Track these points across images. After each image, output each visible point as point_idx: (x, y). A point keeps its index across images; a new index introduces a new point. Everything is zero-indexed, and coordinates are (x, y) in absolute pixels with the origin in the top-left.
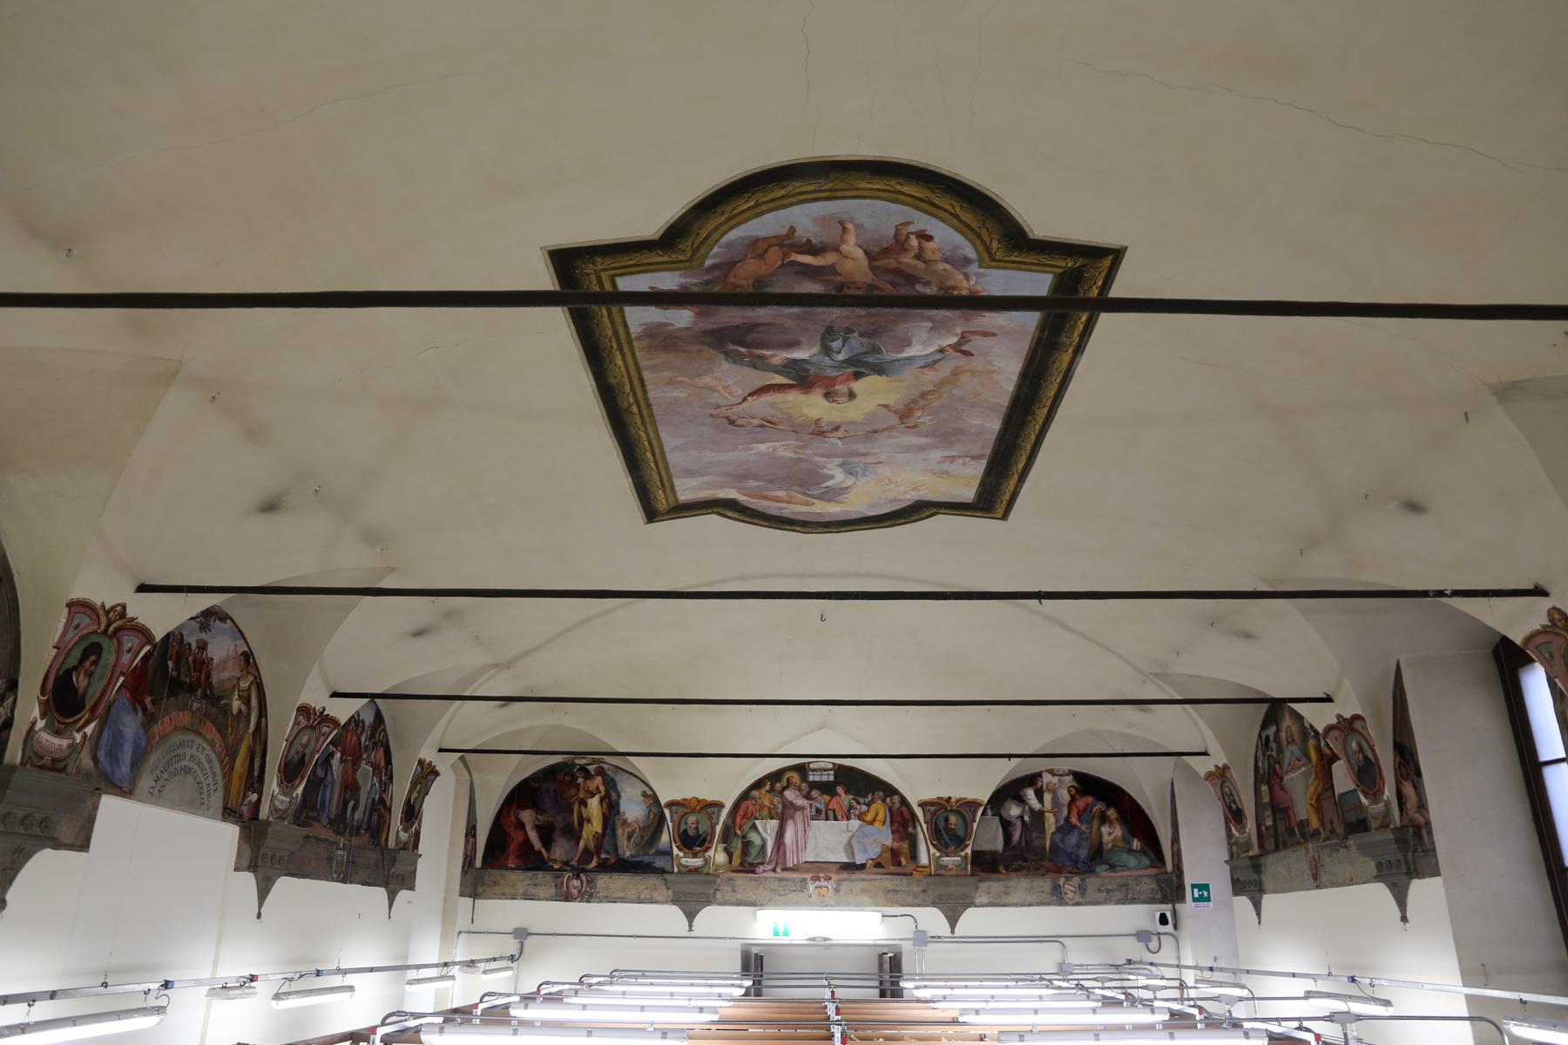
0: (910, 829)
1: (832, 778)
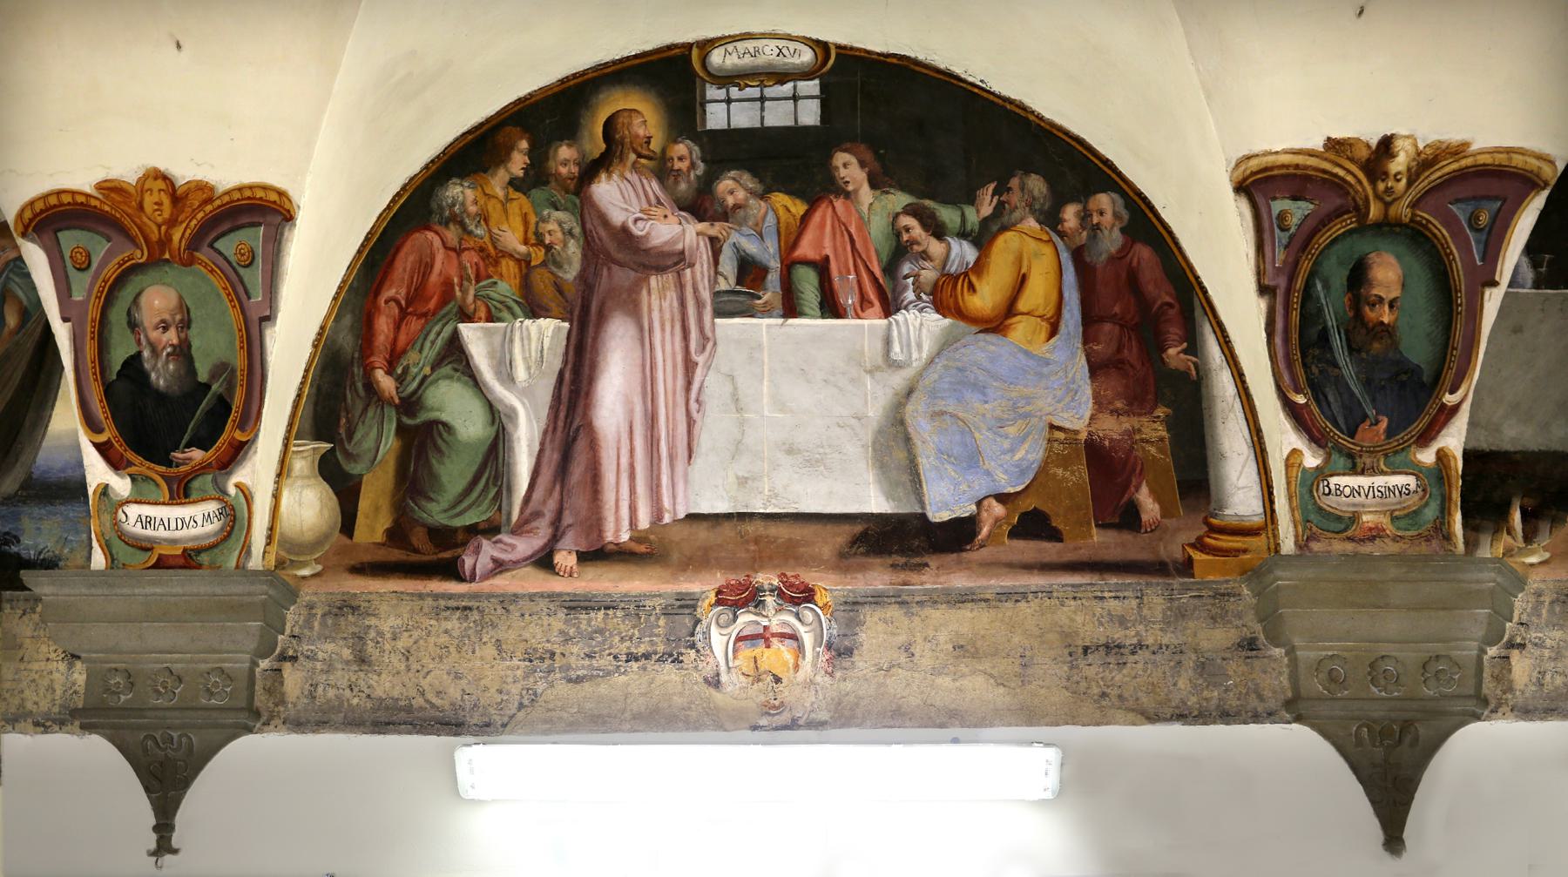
0: (1174, 354)
1: (810, 114)
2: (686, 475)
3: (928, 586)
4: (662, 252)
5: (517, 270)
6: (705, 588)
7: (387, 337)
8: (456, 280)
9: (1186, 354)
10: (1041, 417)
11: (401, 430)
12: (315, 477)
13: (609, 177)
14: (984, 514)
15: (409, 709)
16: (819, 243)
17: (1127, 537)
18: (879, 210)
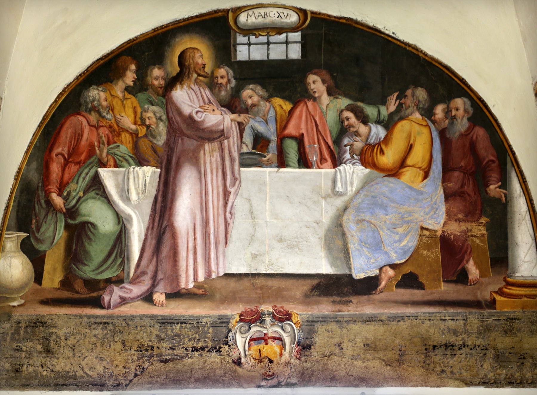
0: (493, 189)
2: (224, 253)
3: (352, 313)
4: (211, 130)
5: (130, 139)
6: (234, 313)
7: (58, 175)
8: (96, 144)
9: (500, 188)
10: (416, 223)
11: (67, 227)
12: (19, 252)
13: (182, 87)
14: (383, 275)
15: (75, 377)
16: (298, 127)
17: (460, 287)
18: (332, 108)
